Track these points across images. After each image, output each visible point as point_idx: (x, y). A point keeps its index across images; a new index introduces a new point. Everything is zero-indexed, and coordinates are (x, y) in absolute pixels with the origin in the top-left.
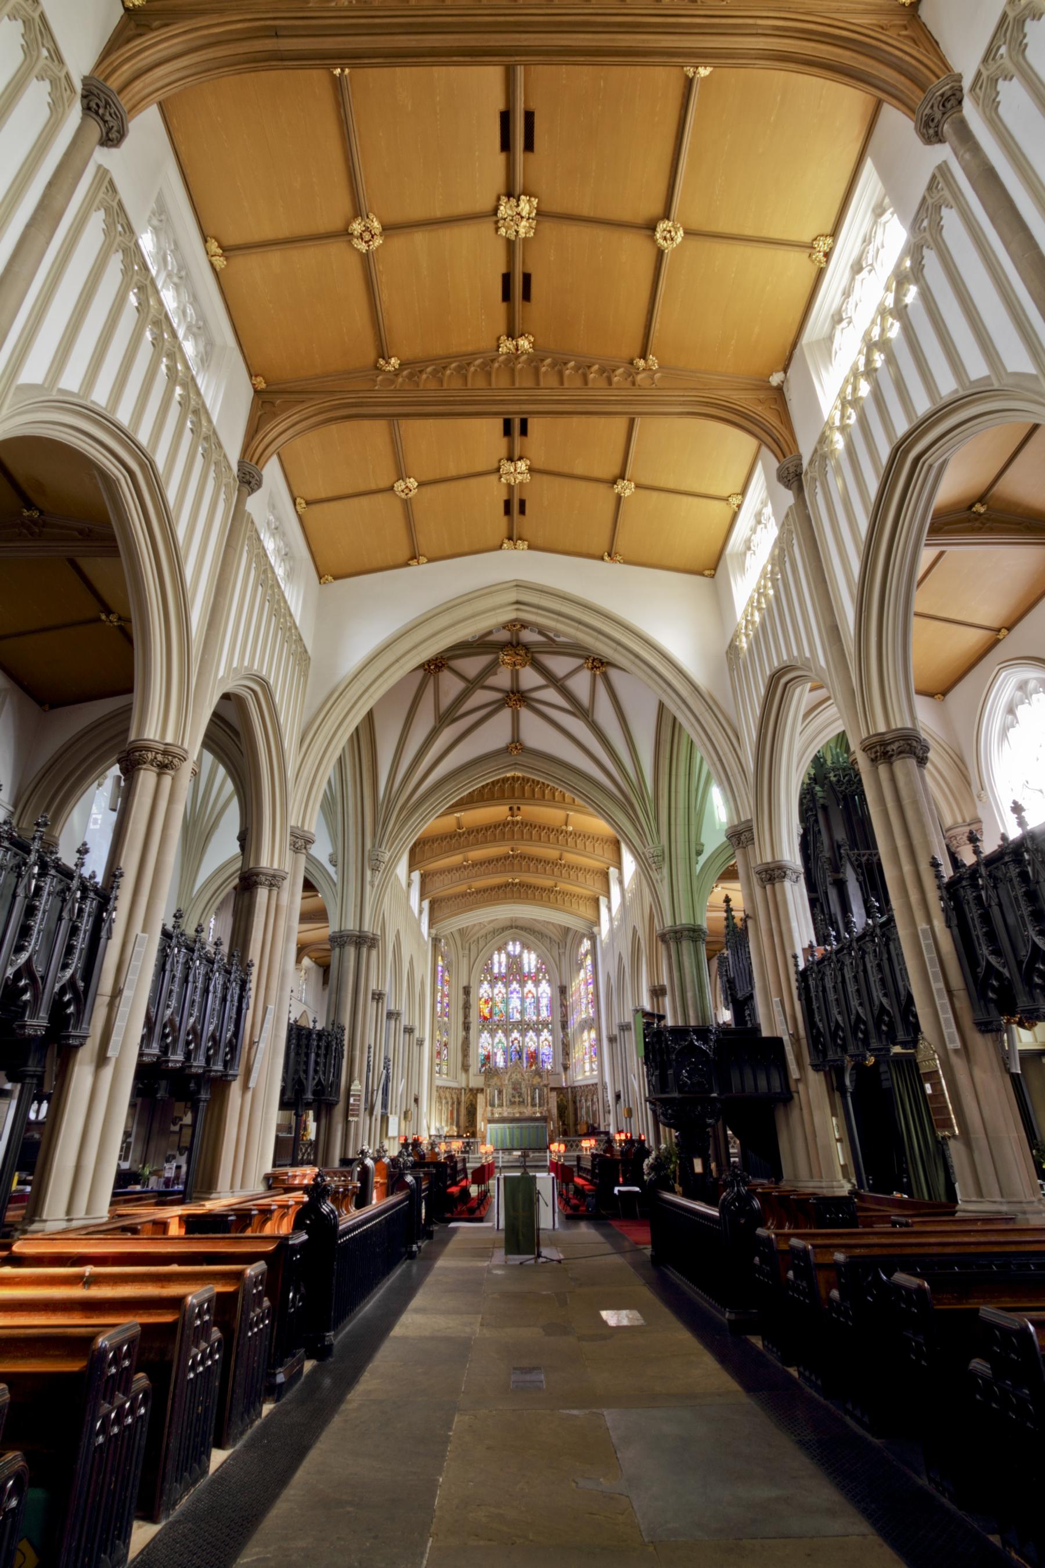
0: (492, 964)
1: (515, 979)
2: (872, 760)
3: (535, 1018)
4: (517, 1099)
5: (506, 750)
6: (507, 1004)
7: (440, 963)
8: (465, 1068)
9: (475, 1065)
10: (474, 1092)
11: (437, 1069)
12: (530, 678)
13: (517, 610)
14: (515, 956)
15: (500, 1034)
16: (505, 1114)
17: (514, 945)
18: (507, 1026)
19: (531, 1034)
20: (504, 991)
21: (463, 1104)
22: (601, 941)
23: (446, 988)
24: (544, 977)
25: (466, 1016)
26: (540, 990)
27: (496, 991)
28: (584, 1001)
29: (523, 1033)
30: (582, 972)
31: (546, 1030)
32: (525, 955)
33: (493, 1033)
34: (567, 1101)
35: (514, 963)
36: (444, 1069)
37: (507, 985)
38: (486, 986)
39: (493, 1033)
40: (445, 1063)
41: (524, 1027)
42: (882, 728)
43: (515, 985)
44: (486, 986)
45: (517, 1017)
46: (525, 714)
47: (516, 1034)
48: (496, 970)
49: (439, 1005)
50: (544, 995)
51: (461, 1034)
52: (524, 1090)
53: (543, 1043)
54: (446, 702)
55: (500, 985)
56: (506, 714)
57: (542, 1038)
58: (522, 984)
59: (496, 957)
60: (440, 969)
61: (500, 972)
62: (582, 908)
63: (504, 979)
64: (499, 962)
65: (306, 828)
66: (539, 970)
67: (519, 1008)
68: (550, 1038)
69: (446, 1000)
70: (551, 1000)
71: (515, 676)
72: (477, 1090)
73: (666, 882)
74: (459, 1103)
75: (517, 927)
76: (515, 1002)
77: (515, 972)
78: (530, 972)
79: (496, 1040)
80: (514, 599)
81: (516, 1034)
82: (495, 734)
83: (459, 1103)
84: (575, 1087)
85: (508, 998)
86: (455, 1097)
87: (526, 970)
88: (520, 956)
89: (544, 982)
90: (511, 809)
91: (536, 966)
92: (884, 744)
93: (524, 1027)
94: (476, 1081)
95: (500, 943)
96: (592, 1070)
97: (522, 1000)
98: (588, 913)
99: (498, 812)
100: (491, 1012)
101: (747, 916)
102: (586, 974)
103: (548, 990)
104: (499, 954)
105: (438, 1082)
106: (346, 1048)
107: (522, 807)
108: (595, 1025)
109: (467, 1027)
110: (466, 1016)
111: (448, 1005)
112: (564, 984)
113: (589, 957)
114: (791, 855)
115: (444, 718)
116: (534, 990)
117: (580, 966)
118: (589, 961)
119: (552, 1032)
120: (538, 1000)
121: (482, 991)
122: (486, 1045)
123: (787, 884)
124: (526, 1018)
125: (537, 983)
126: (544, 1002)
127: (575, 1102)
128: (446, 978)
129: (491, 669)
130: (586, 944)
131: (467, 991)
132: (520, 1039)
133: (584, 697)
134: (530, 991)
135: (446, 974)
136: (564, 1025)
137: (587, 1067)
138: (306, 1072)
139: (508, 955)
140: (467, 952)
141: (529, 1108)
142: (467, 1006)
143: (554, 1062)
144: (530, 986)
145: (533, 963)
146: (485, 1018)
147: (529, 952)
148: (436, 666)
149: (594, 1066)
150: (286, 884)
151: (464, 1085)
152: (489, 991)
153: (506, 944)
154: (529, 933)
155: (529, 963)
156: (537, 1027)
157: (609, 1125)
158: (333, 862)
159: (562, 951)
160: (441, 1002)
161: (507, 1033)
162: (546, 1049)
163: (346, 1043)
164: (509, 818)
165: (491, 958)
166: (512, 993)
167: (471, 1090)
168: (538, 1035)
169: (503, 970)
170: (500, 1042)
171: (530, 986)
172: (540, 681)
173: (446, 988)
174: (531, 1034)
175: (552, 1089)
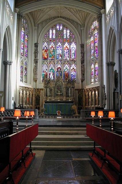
0: (49, 34)
4: (59, 93)
8: (35, 80)
9: (40, 78)
14: (59, 30)
16: (54, 100)
25: (36, 56)
26: (71, 46)
27: (50, 46)
28: (93, 51)
32: (65, 31)
35: (59, 34)
37: (56, 44)
43: (59, 44)
44: (46, 44)
48: (51, 37)
51: (33, 65)
53: (73, 70)
58: (63, 44)
59: (51, 31)
64: (52, 34)
70: (76, 51)
72: (41, 89)
75: (61, 17)
87: (65, 37)
88: (62, 31)
93: (63, 62)
97: (63, 51)
100: (48, 56)
103: (75, 46)
109: (36, 62)
110: (36, 56)
111: (27, 51)
116: (68, 47)
117: (92, 34)
118: (96, 32)
120: (70, 51)
126: (73, 52)
131: (36, 45)
134: (66, 47)
137: (93, 80)
139: (56, 30)
141: (65, 97)
144: (66, 44)
145: (68, 34)
153: (56, 26)
156: (70, 63)
157: (105, 105)
165: (49, 31)
171: (66, 44)
173: (26, 43)
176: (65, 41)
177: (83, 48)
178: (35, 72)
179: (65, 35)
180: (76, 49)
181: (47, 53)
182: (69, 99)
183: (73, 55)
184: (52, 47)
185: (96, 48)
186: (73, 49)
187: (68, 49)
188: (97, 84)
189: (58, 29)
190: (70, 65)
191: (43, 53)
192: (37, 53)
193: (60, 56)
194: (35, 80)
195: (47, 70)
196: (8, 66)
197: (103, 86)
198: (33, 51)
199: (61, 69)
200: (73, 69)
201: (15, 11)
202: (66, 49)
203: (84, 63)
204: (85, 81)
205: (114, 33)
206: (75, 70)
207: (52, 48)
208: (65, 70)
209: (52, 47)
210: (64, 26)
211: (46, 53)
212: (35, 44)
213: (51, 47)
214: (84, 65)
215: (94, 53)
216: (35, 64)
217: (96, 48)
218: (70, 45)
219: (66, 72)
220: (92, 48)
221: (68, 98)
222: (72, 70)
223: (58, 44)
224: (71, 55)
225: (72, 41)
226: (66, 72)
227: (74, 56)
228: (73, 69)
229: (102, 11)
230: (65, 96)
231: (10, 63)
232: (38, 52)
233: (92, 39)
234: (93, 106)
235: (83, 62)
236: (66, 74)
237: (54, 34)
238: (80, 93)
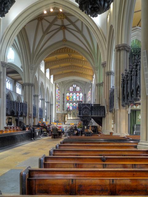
2: (117, 51)
5: (63, 41)
7: (57, 89)
8: (63, 110)
9: (65, 109)
12: (66, 22)
13: (55, 5)
15: (71, 104)
17: (75, 85)
20: (72, 95)
25: (64, 100)
27: (70, 95)
32: (77, 87)
33: (69, 103)
35: (75, 90)
36: (59, 110)
38: (68, 94)
42: (120, 44)
44: (68, 94)
45: (75, 100)
46: (66, 31)
47: (74, 103)
48: (70, 90)
49: (57, 98)
51: (62, 103)
52: (76, 114)
54: (45, 29)
55: (71, 94)
56: (61, 32)
58: (76, 94)
59: (70, 88)
60: (57, 90)
62: (89, 78)
63: (72, 92)
64: (71, 89)
65: (5, 62)
66: (80, 90)
71: (63, 21)
73: (98, 73)
74: (62, 116)
76: (74, 97)
77: (75, 91)
78: (78, 91)
80: (53, 2)
81: (74, 103)
82: (59, 37)
83: (62, 116)
87: (77, 90)
90: (69, 55)
92: (119, 47)
94: (65, 112)
95: (70, 85)
97: (76, 97)
99: (65, 55)
101: (103, 82)
105: (57, 112)
106: (28, 106)
107: (72, 55)
109: (64, 102)
110: (64, 100)
114: (113, 69)
115: (45, 32)
116: (79, 95)
120: (80, 97)
121: (67, 95)
123: (112, 76)
125: (79, 93)
126: (81, 97)
129: (55, 19)
130: (90, 86)
131: (64, 95)
133: (80, 28)
135: (59, 91)
138: (18, 110)
139: (73, 87)
142: (64, 98)
144: (78, 94)
145: (79, 89)
146: (68, 100)
147: (78, 87)
148: (41, 19)
150: (2, 74)
152: (69, 95)
154: (77, 83)
158: (22, 67)
161: (73, 103)
163: (28, 105)
165: (69, 88)
169: (72, 90)
171: (78, 94)
172: (69, 23)
179: (77, 90)
194: (63, 110)
201: (54, 83)
210: (77, 85)
218: (79, 94)
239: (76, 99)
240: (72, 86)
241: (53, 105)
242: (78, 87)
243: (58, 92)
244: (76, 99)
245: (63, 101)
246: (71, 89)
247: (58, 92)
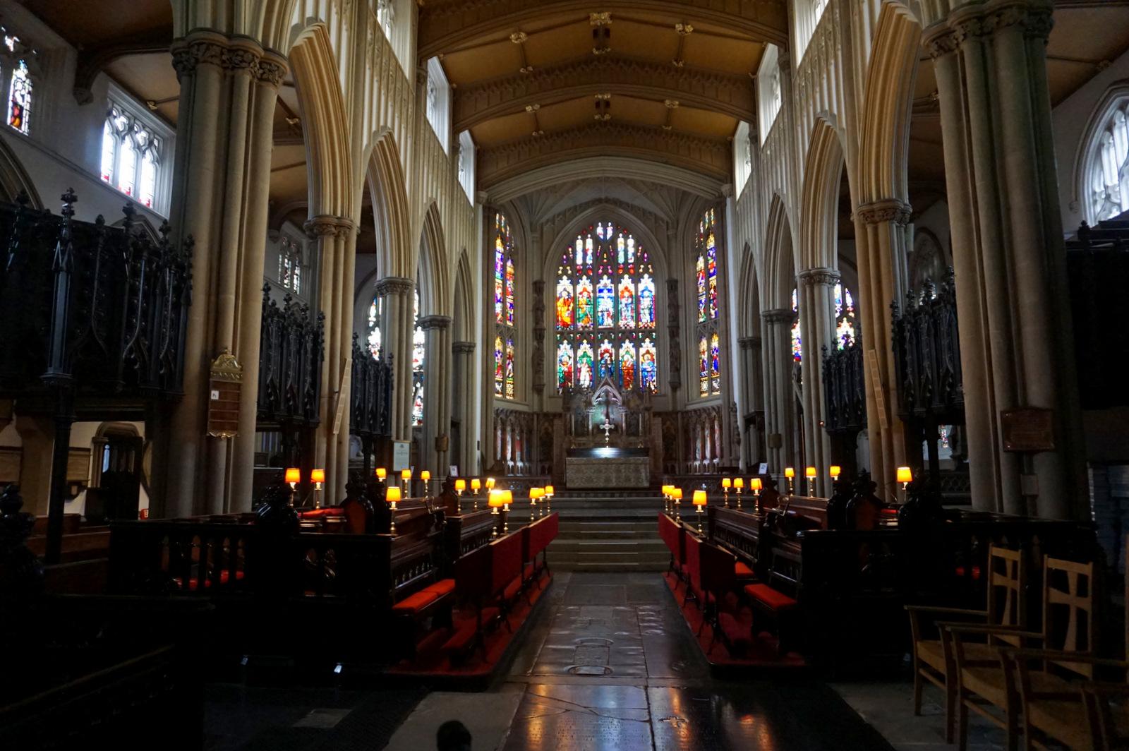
0: (574, 252)
1: (605, 272)
3: (632, 324)
6: (595, 306)
7: (499, 246)
8: (538, 389)
10: (549, 417)
11: (498, 387)
15: (585, 347)
18: (595, 336)
19: (627, 345)
20: (590, 288)
21: (535, 432)
22: (734, 203)
23: (510, 283)
24: (646, 270)
26: (641, 287)
27: (579, 288)
28: (703, 299)
29: (617, 344)
30: (701, 260)
31: (647, 340)
32: (621, 241)
33: (575, 345)
34: (676, 430)
35: (605, 250)
36: (510, 389)
37: (595, 280)
39: (575, 345)
40: (510, 381)
41: (618, 336)
43: (605, 281)
45: (608, 322)
47: (606, 345)
48: (579, 261)
49: (498, 307)
50: (646, 293)
51: (531, 344)
53: (643, 357)
55: (585, 283)
57: (642, 351)
58: (616, 280)
59: (579, 243)
60: (498, 256)
61: (584, 264)
64: (583, 250)
66: (639, 260)
67: (612, 310)
68: (653, 350)
69: (509, 300)
70: (656, 300)
74: (530, 432)
76: (606, 304)
77: (606, 263)
78: (626, 263)
79: (580, 353)
81: (606, 345)
83: (530, 432)
84: (687, 412)
85: (595, 298)
86: (523, 423)
87: (621, 260)
89: (646, 276)
91: (634, 254)
93: (618, 336)
96: (711, 389)
97: (616, 301)
98: (717, 165)
102: (706, 262)
103: (652, 286)
104: (584, 240)
105: (497, 405)
108: (721, 326)
109: (539, 335)
112: (675, 277)
113: (712, 238)
117: (701, 250)
118: (711, 243)
119: (655, 342)
120: (637, 300)
121: (560, 288)
122: (565, 359)
124: (621, 323)
125: (636, 279)
127: (686, 431)
128: (510, 269)
130: (710, 217)
131: (538, 287)
132: (613, 351)
134: (626, 288)
135: (509, 263)
136: (674, 332)
137: (705, 386)
140: (537, 235)
141: (624, 437)
143: (659, 381)
144: (626, 281)
145: (631, 250)
146: (565, 325)
147: (626, 238)
149: (715, 384)
151: (536, 409)
152: (570, 288)
155: (626, 252)
156: (636, 336)
157: (738, 460)
159: (670, 233)
160: (503, 302)
161: (595, 345)
162: (646, 364)
164: (596, 52)
165: (573, 246)
166: (601, 291)
167: (546, 415)
168: (637, 346)
169: (589, 261)
170: (585, 354)
171: (626, 281)
173: (510, 283)
174: (627, 345)
175: (657, 414)
176: (621, 272)
177: (676, 288)
178: (539, 364)
180: (653, 293)
181: (571, 308)
182: (636, 444)
183: (647, 312)
184: (585, 290)
185: (712, 291)
186: (646, 293)
187: (631, 296)
188: (717, 398)
189: (602, 237)
190: (638, 345)
191: (559, 309)
192: (542, 311)
193: (608, 315)
195: (570, 358)
196: (464, 356)
197: (731, 406)
198: (530, 307)
199: (611, 356)
200: (648, 352)
202: (626, 294)
203: (678, 335)
204: (682, 388)
205: (787, 218)
206: (652, 356)
207: (585, 294)
208: (623, 357)
209: (585, 290)
211: (568, 310)
212: (535, 284)
213: (581, 290)
214: (678, 345)
215: (707, 309)
216: (535, 343)
217: (712, 291)
219: (625, 362)
220: (700, 290)
221: (632, 439)
222: (643, 356)
223: (603, 282)
224: (642, 312)
225: (641, 270)
226: (625, 362)
227: (650, 314)
228: (648, 352)
229: (725, 188)
230: (625, 433)
231: (470, 347)
232: (543, 306)
233: (701, 264)
234: (706, 462)
235: (674, 332)
236: (628, 369)
237: (590, 252)
238: (668, 423)
239: (616, 316)
240: (586, 231)
241: (470, 348)
242: (626, 238)
243: (504, 267)
244: (616, 316)
245: (535, 330)
246: (585, 252)
247: (504, 267)
